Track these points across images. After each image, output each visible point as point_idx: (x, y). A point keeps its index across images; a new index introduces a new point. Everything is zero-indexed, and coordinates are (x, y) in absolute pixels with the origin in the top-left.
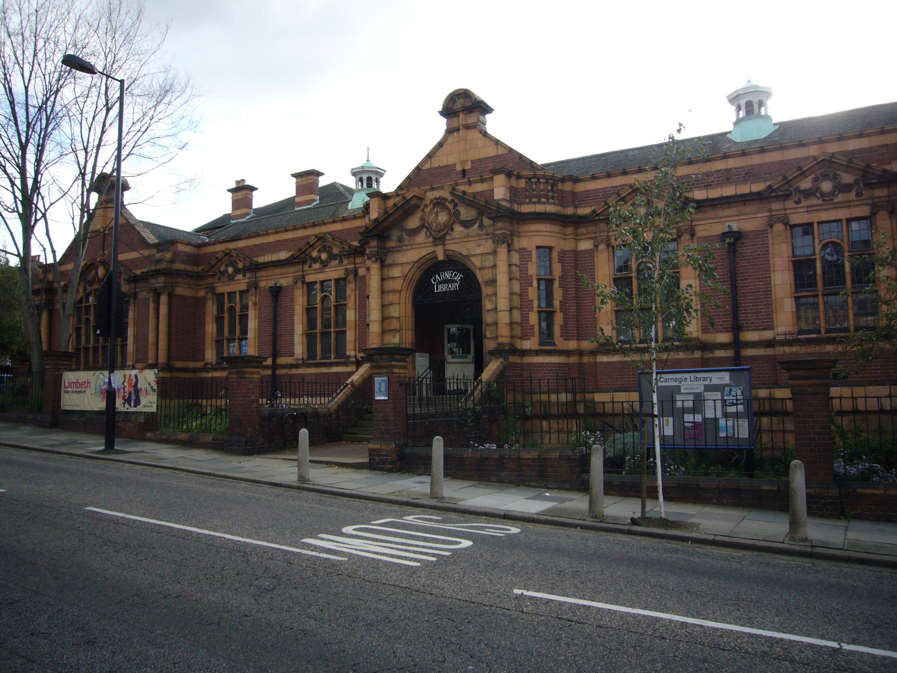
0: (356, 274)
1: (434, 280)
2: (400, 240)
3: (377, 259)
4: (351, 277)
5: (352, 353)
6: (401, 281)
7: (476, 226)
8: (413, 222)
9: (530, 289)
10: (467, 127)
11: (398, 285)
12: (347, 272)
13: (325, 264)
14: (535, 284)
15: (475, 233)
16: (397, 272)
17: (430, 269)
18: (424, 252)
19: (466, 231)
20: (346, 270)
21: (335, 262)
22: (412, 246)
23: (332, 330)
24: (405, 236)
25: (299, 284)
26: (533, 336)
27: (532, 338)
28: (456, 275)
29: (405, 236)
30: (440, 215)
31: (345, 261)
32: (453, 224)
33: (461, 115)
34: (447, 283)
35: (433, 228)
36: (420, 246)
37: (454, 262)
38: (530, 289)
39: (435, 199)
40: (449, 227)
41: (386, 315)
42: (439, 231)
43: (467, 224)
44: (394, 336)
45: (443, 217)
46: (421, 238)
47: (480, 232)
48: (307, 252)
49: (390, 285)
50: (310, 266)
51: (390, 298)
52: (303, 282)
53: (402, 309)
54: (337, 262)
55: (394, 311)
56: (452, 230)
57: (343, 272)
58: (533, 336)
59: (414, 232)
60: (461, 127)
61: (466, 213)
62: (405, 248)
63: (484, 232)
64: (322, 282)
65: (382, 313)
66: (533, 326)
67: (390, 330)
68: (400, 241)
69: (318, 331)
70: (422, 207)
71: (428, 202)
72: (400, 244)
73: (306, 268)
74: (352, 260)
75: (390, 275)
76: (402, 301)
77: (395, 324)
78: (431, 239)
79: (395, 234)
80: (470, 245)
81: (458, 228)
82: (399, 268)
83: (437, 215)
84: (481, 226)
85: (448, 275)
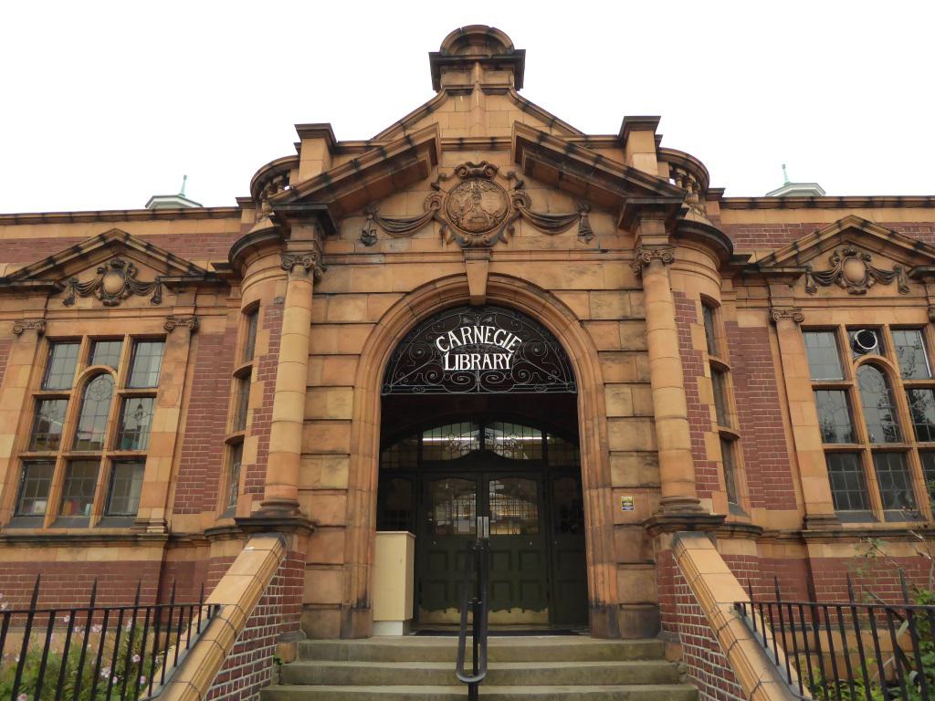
0: (194, 331)
1: (445, 343)
2: (367, 239)
3: (308, 270)
4: (182, 334)
5: (157, 514)
6: (363, 333)
7: (573, 231)
8: (409, 206)
9: (698, 378)
10: (488, 90)
11: (356, 340)
12: (172, 324)
13: (112, 301)
14: (708, 373)
15: (571, 246)
16: (353, 311)
17: (450, 308)
18: (435, 272)
19: (548, 239)
20: (170, 318)
21: (137, 301)
22: (399, 259)
23: (104, 453)
24: (380, 234)
25: (30, 337)
26: (717, 488)
27: (715, 493)
28: (502, 337)
29: (380, 234)
30: (484, 195)
31: (169, 299)
32: (513, 220)
33: (477, 69)
34: (477, 352)
35: (465, 223)
36: (420, 258)
37: (502, 306)
38: (699, 378)
39: (470, 164)
40: (505, 223)
41: (316, 414)
42: (477, 232)
43: (551, 225)
44: (332, 469)
45: (491, 203)
46: (428, 239)
47: (582, 245)
48: (68, 271)
49: (331, 340)
50: (69, 302)
51: (329, 370)
52: (41, 334)
53: (357, 404)
54: (146, 300)
55: (340, 404)
56: (512, 232)
57: (162, 322)
58: (717, 488)
59: (409, 228)
60: (477, 86)
61: (542, 201)
62: (375, 259)
63: (593, 245)
64: (94, 340)
65: (306, 404)
66: (714, 464)
67: (320, 454)
68: (367, 244)
69: (59, 454)
70: (433, 178)
71: (449, 173)
72: (368, 250)
73: (56, 304)
74: (187, 298)
75: (331, 318)
76: (361, 382)
77: (337, 438)
78: (454, 247)
79: (353, 230)
80: (558, 269)
81: (526, 232)
82: (361, 303)
83: (477, 195)
84: (586, 232)
85: (480, 335)
